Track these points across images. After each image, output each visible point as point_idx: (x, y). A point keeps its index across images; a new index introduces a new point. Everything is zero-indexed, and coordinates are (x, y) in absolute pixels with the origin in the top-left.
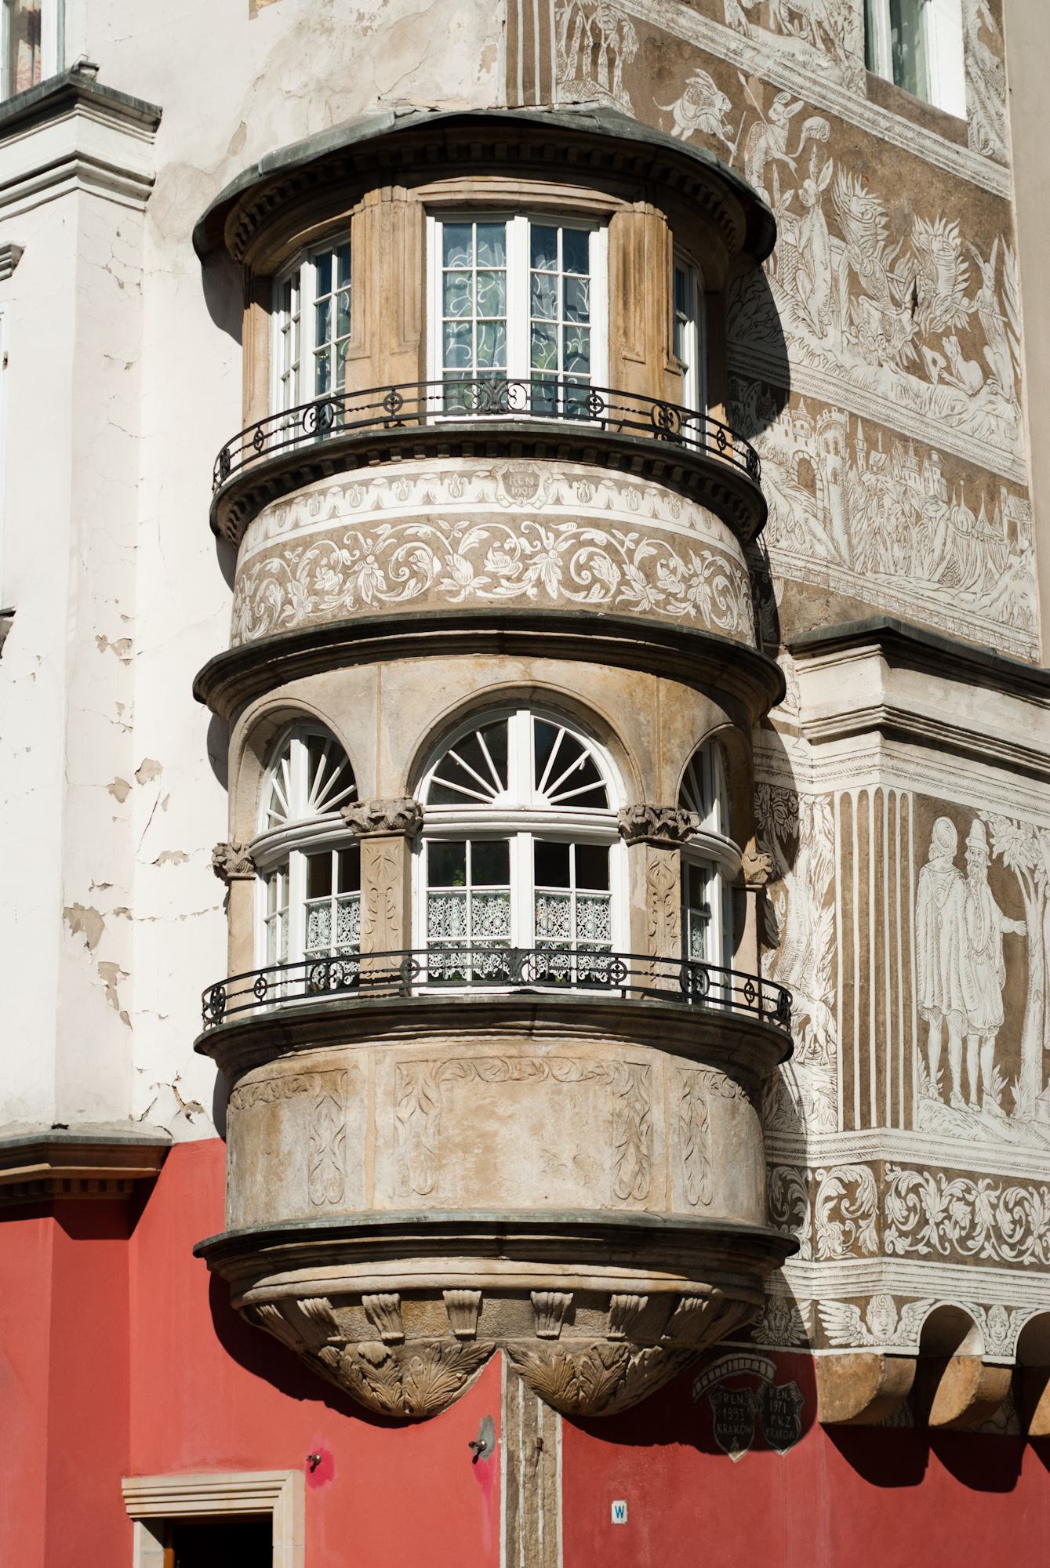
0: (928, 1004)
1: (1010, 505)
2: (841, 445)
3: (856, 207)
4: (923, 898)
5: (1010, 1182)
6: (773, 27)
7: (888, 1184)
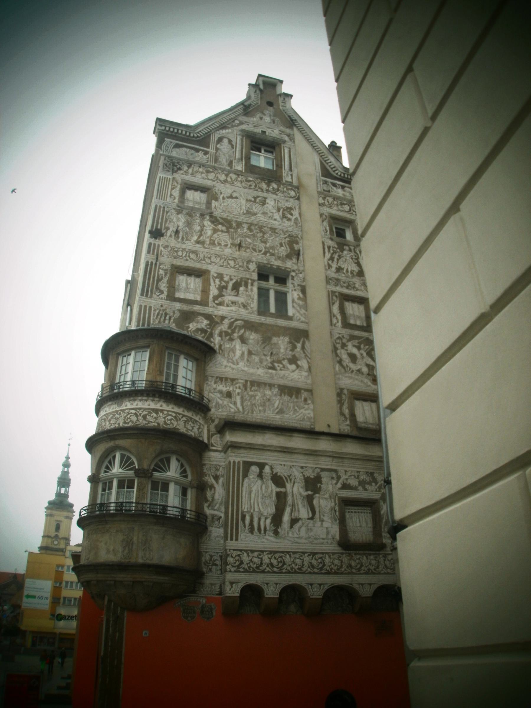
0: (246, 510)
1: (304, 395)
2: (241, 387)
3: (251, 337)
5: (276, 552)
6: (225, 305)
7: (228, 555)
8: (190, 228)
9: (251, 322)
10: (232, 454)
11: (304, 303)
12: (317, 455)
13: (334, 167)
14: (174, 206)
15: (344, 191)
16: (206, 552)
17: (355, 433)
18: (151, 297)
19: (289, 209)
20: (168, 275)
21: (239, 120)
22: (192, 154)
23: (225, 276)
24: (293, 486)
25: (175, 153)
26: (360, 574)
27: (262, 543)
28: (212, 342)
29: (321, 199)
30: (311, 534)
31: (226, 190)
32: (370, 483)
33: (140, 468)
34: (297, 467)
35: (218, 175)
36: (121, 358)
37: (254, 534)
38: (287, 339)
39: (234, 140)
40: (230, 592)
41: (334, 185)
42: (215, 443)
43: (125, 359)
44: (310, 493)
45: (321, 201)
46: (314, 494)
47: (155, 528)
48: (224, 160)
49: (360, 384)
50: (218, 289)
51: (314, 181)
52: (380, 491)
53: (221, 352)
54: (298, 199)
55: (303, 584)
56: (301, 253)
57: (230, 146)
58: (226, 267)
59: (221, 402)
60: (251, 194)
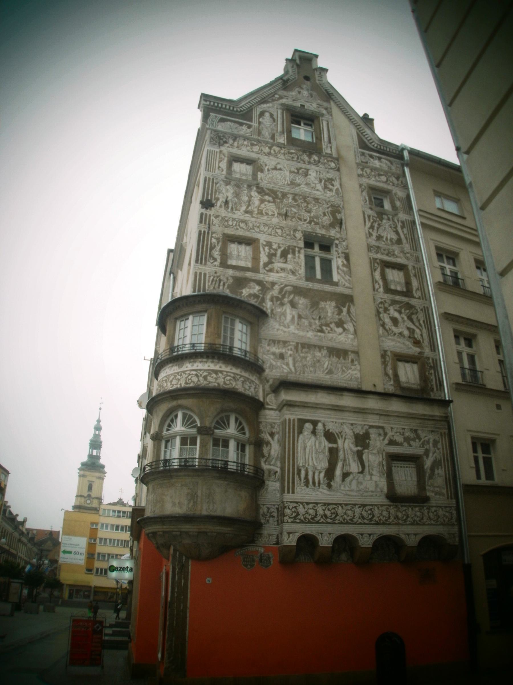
0: (301, 465)
1: (351, 356)
2: (293, 349)
3: (301, 302)
4: (300, 441)
5: (329, 504)
6: (275, 271)
7: (286, 507)
8: (239, 199)
9: (300, 287)
10: (287, 412)
11: (348, 269)
12: (365, 413)
13: (371, 139)
14: (223, 177)
15: (381, 162)
16: (264, 505)
17: (399, 392)
18: (205, 264)
19: (330, 180)
20: (220, 243)
21: (278, 95)
22: (236, 128)
23: (273, 244)
24: (344, 442)
25: (221, 127)
26: (406, 525)
27: (316, 496)
28: (264, 307)
29: (359, 170)
30: (361, 487)
31: (270, 162)
32: (414, 440)
33: (203, 426)
34: (347, 424)
35: (262, 148)
36: (179, 322)
37: (309, 487)
38: (333, 304)
39: (275, 114)
40: (287, 541)
41: (371, 156)
42: (270, 402)
43: (183, 323)
44: (359, 448)
45: (360, 172)
46: (364, 449)
47: (218, 481)
48: (266, 134)
49: (402, 346)
50: (268, 256)
51: (352, 153)
52: (423, 447)
53: (273, 316)
54: (339, 170)
55: (355, 534)
56: (343, 222)
57: (271, 119)
58: (274, 236)
59: (274, 363)
60: (294, 165)
